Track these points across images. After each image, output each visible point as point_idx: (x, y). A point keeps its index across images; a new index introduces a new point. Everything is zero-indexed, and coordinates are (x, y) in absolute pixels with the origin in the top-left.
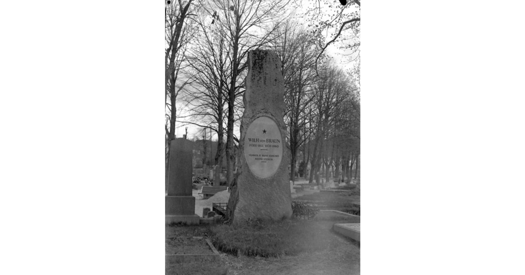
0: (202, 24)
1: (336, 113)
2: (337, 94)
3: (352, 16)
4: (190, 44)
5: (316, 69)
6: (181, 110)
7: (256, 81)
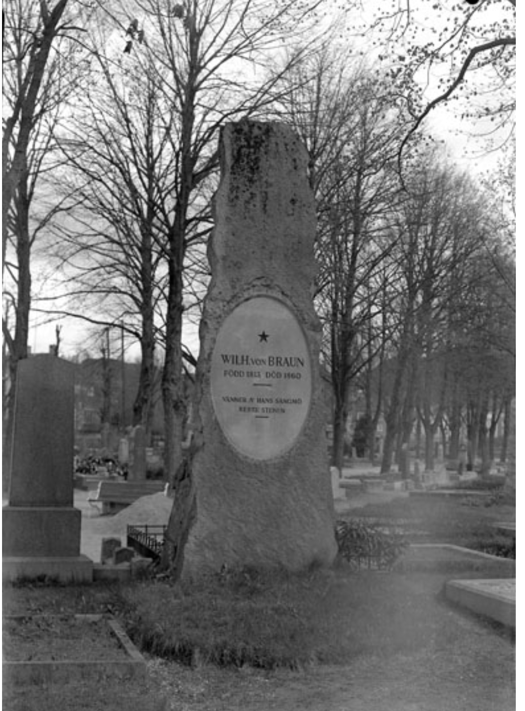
0: (100, 52)
1: (452, 289)
2: (455, 239)
3: (493, 31)
4: (68, 107)
5: (399, 173)
6: (43, 281)
7: (242, 203)
